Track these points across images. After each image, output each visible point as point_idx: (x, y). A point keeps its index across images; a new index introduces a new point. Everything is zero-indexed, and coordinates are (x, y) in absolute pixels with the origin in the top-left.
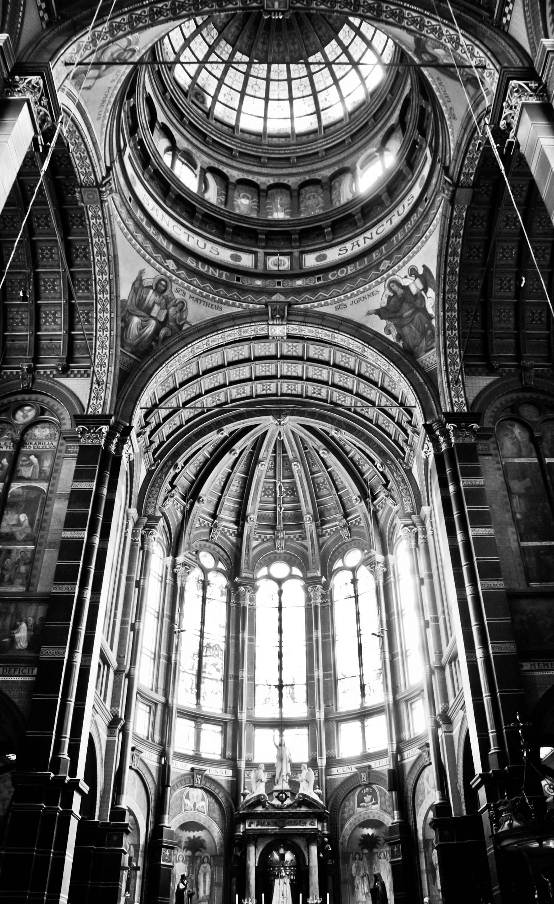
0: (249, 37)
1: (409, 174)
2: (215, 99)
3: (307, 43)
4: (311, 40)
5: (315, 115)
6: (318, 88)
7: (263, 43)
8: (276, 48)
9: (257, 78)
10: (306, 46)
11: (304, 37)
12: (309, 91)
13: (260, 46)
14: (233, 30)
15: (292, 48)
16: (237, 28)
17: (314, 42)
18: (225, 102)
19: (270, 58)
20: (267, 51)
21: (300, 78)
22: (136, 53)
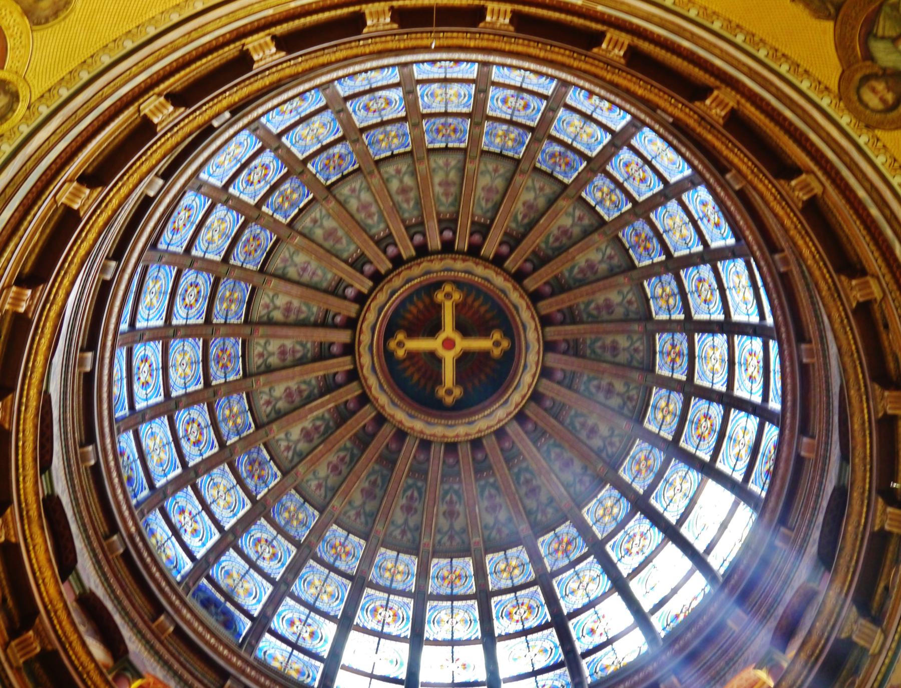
0: (368, 494)
1: (871, 640)
2: (261, 624)
3: (531, 504)
4: (543, 498)
5: (564, 670)
6: (566, 606)
7: (408, 509)
8: (444, 523)
9: (389, 590)
10: (529, 513)
11: (523, 490)
12: (545, 615)
13: (399, 517)
14: (323, 471)
15: (489, 520)
16: (335, 468)
17: (551, 500)
18: (293, 639)
19: (426, 541)
20: (418, 528)
21: (514, 589)
22: (21, 109)
